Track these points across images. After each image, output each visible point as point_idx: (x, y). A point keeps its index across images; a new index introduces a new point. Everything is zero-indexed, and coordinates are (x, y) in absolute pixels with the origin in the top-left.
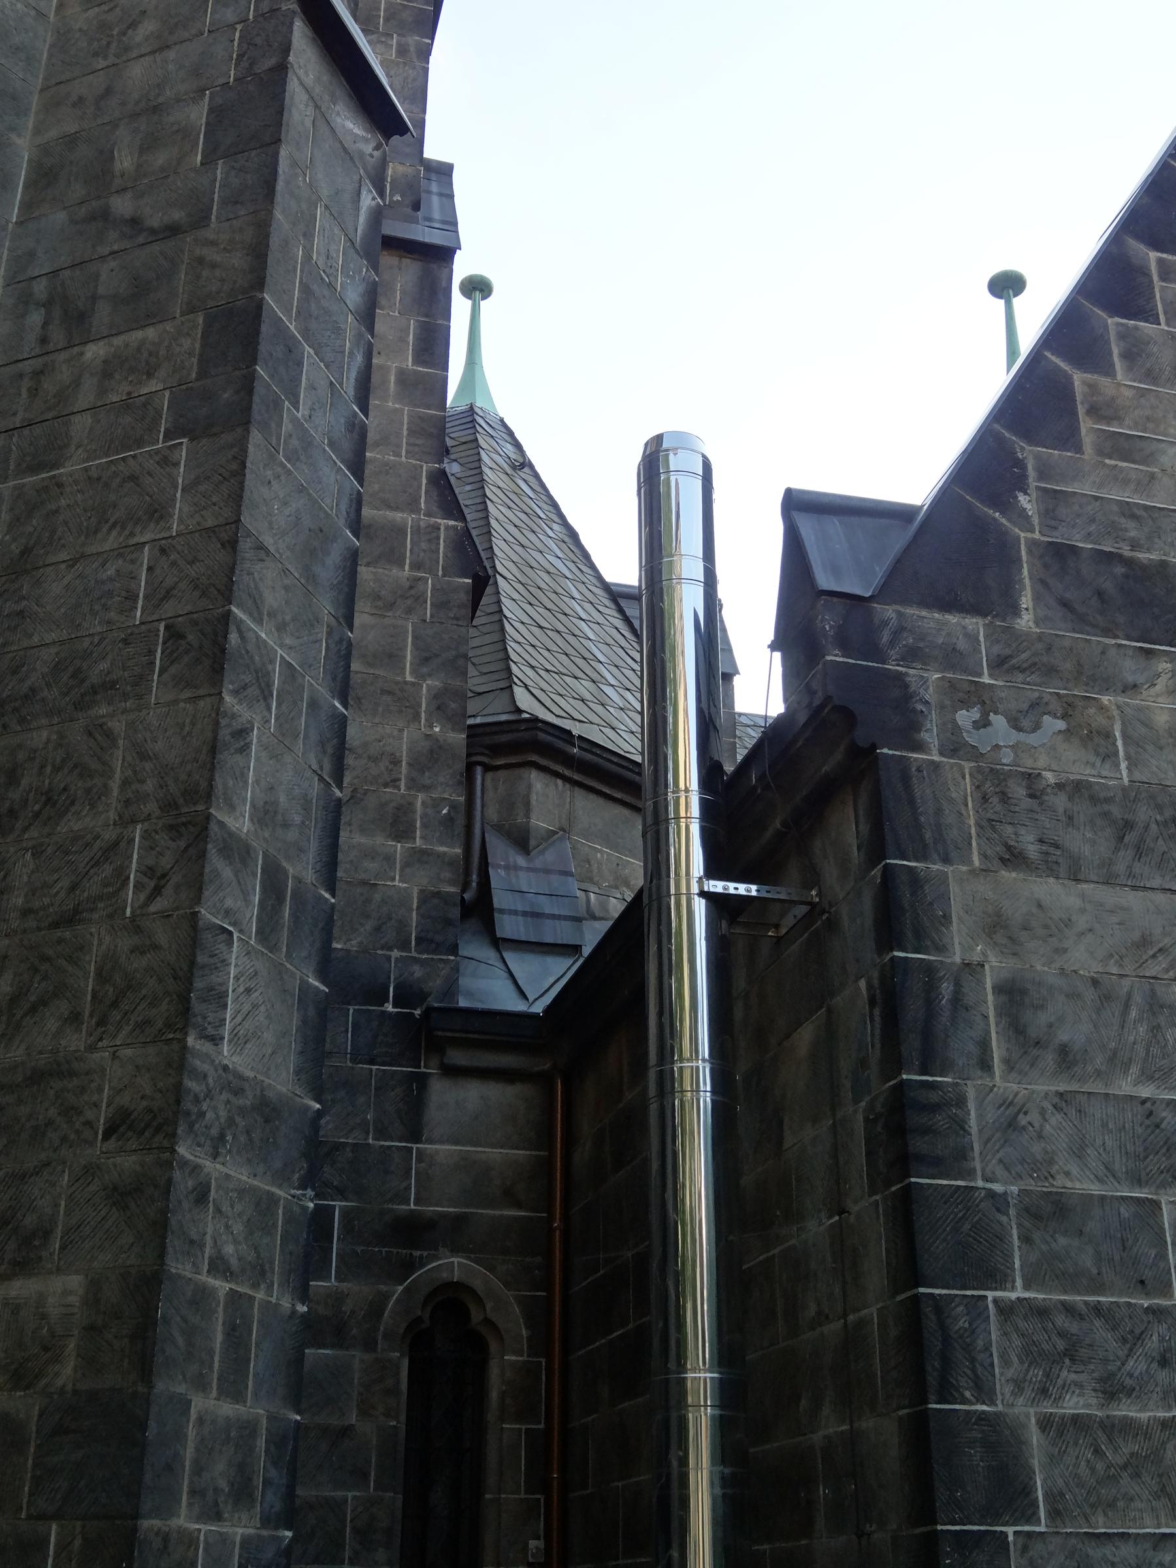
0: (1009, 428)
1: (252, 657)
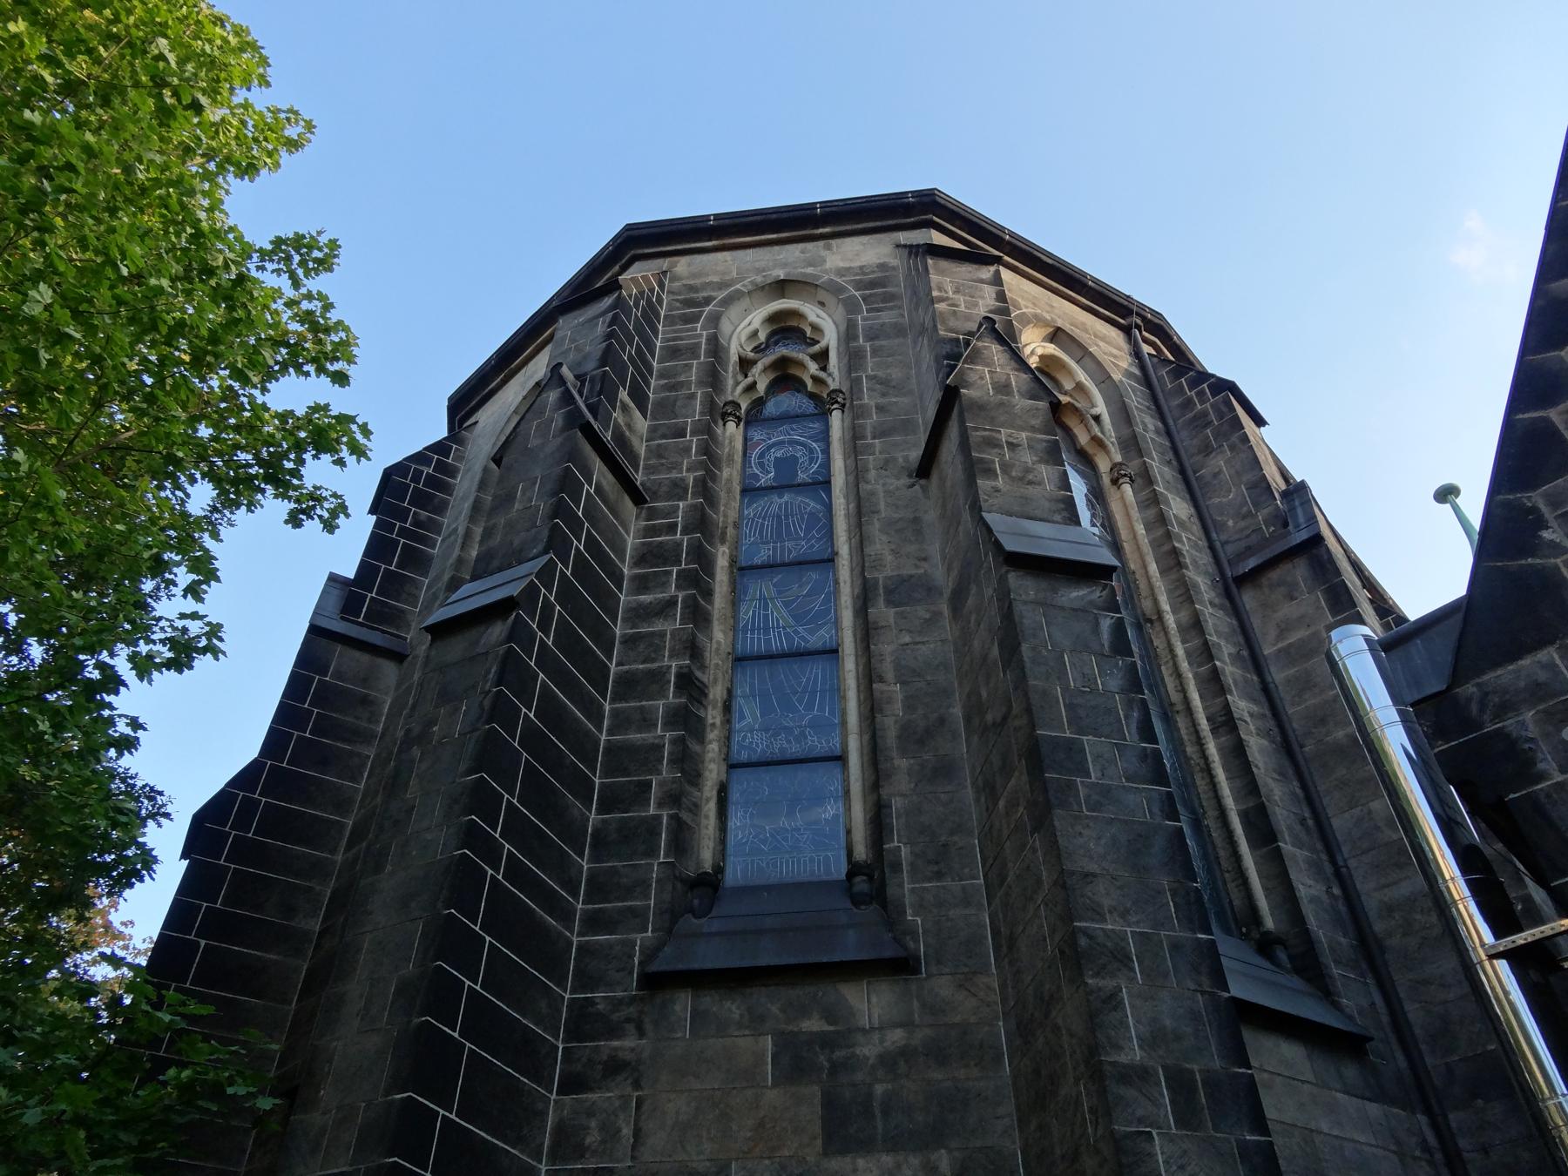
0: (1511, 491)
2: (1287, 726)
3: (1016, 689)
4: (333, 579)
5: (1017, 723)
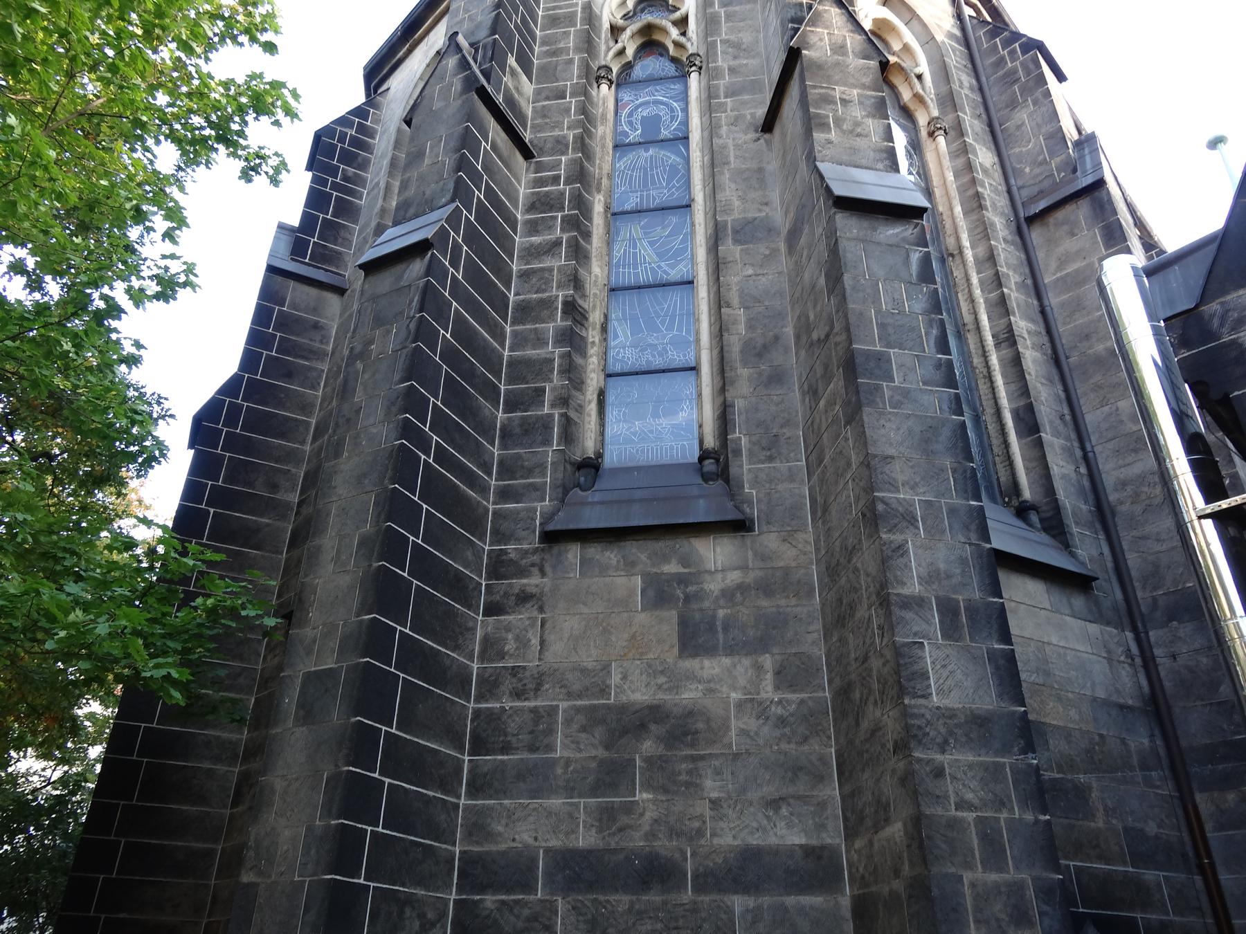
1: (897, 510)
2: (1057, 341)
3: (837, 311)
4: (282, 227)
5: (838, 339)
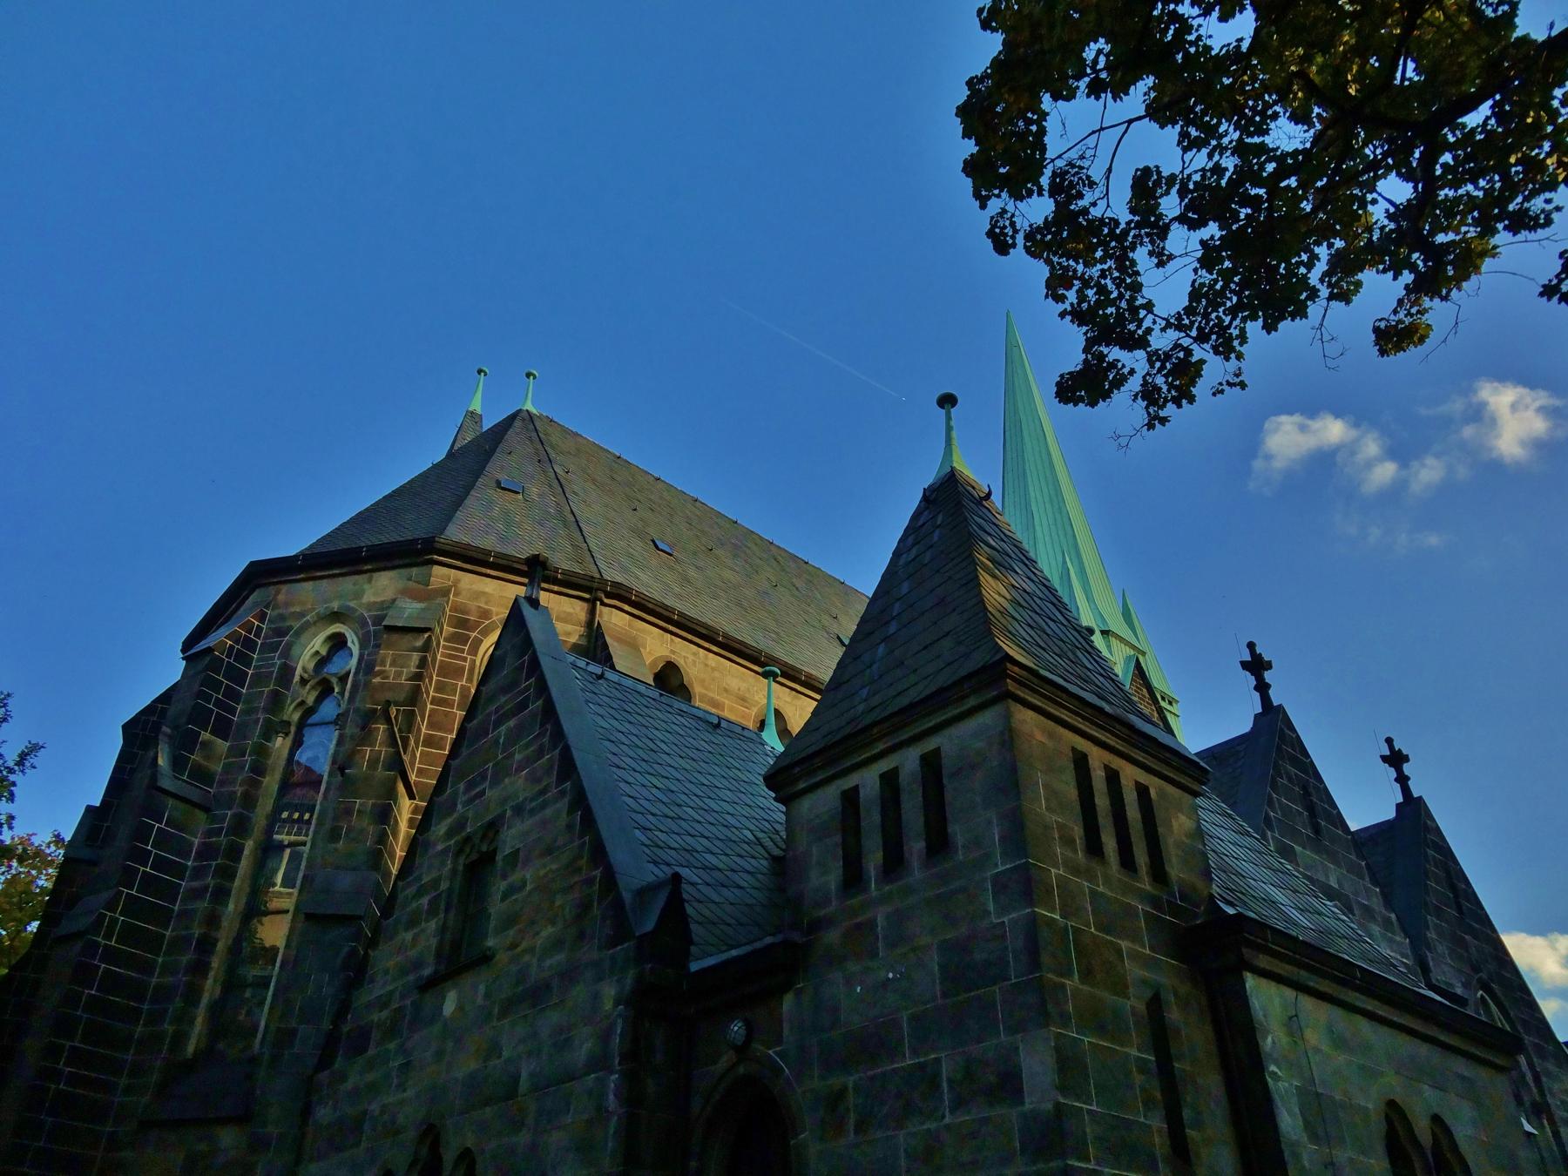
4: (89, 809)
